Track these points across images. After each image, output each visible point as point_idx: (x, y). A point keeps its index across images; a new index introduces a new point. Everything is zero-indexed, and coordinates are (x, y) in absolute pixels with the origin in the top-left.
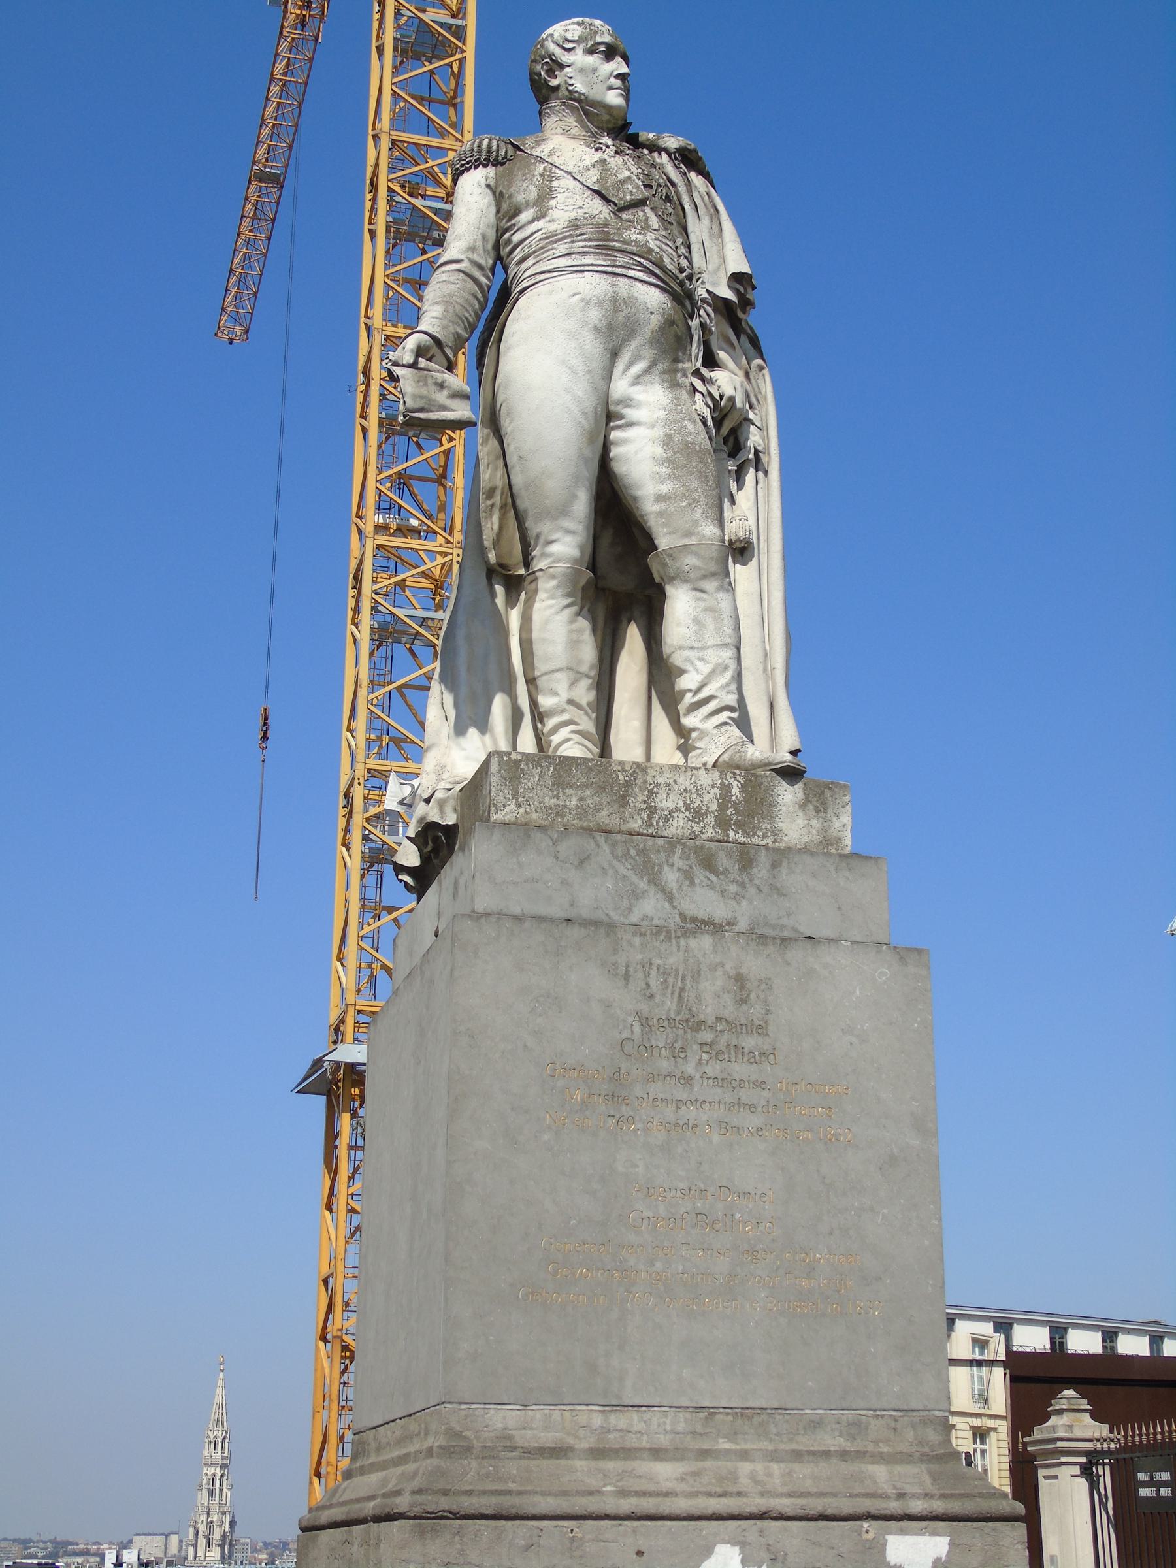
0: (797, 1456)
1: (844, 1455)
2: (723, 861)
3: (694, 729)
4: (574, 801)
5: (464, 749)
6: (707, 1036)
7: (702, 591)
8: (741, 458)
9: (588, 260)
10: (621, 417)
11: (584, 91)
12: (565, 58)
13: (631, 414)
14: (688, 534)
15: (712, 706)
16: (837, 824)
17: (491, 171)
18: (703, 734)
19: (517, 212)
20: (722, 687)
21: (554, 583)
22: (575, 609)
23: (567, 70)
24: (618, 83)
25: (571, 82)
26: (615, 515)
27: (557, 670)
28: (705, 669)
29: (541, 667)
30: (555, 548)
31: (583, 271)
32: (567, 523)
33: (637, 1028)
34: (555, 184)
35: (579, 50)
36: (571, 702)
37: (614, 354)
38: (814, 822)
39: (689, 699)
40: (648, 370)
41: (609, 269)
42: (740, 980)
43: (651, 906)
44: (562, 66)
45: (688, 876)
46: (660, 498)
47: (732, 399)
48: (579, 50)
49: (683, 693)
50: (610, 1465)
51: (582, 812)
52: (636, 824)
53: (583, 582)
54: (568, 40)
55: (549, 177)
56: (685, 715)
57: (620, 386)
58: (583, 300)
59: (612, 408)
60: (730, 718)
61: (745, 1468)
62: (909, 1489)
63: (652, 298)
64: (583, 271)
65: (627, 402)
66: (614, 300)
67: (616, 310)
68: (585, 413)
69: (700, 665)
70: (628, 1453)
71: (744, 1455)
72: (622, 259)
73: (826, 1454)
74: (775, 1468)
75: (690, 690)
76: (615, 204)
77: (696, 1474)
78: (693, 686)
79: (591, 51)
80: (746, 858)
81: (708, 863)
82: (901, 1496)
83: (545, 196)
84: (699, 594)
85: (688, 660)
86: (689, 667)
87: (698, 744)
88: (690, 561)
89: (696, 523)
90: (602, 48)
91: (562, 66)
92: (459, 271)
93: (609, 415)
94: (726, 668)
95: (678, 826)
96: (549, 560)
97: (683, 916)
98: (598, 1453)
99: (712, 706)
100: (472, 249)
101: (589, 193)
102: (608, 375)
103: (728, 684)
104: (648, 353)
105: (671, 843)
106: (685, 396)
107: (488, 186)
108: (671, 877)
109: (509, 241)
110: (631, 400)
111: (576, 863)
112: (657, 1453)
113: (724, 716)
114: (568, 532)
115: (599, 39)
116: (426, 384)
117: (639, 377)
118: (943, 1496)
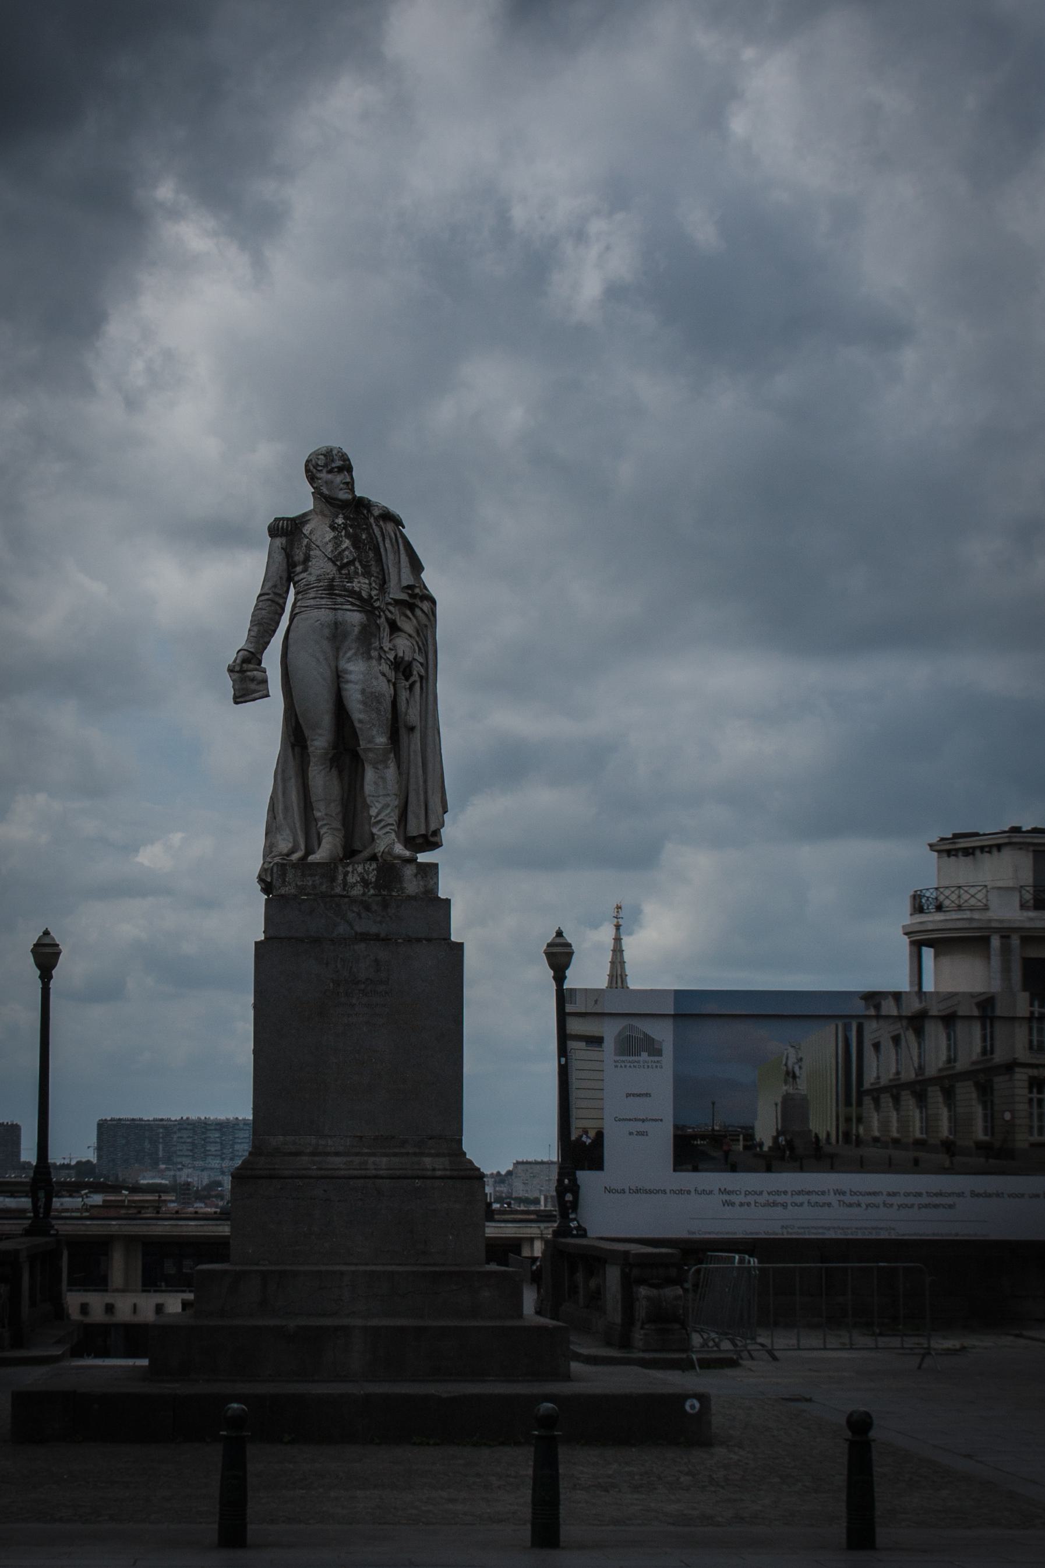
0: (395, 1155)
1: (415, 1154)
2: (374, 907)
4: (310, 883)
6: (362, 986)
8: (412, 679)
9: (323, 602)
12: (318, 475)
14: (370, 742)
15: (382, 824)
17: (283, 540)
19: (295, 566)
24: (344, 486)
28: (379, 806)
29: (313, 799)
30: (316, 743)
33: (331, 985)
34: (312, 553)
35: (324, 471)
36: (326, 815)
37: (337, 650)
38: (421, 883)
39: (373, 820)
40: (355, 654)
42: (376, 960)
43: (342, 929)
45: (359, 915)
46: (360, 721)
48: (324, 471)
50: (316, 1159)
51: (314, 887)
52: (338, 890)
53: (330, 756)
55: (308, 547)
57: (343, 664)
61: (372, 1159)
62: (437, 1167)
63: (355, 618)
65: (346, 672)
66: (336, 623)
67: (336, 628)
70: (328, 1154)
71: (373, 1155)
72: (340, 600)
73: (408, 1154)
74: (384, 1159)
77: (877, 1046)
79: (330, 472)
80: (385, 905)
81: (368, 908)
82: (434, 1170)
83: (307, 559)
88: (371, 755)
89: (373, 737)
92: (268, 600)
93: (339, 677)
95: (357, 891)
97: (356, 933)
98: (313, 1154)
99: (382, 824)
100: (275, 586)
102: (337, 658)
104: (354, 645)
105: (353, 900)
106: (374, 662)
108: (351, 916)
112: (337, 1154)
113: (387, 829)
114: (320, 735)
115: (334, 465)
118: (451, 1170)
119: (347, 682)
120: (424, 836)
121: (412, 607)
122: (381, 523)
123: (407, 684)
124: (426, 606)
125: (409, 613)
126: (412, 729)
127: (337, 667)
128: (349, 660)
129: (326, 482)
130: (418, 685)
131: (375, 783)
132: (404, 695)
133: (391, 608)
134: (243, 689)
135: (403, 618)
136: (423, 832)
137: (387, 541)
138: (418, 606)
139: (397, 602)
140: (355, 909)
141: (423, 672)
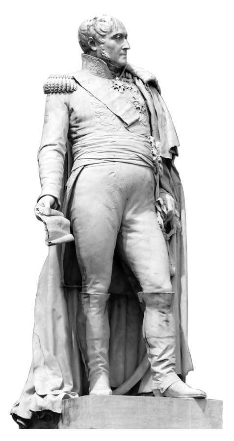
3: (158, 373)
5: (52, 370)
7: (163, 313)
10: (129, 227)
11: (109, 57)
12: (102, 40)
13: (134, 227)
18: (162, 375)
20: (170, 355)
21: (96, 301)
23: (102, 45)
25: (104, 52)
26: (123, 268)
28: (164, 347)
44: (100, 43)
47: (171, 212)
49: (152, 356)
54: (102, 31)
56: (153, 366)
57: (129, 215)
58: (115, 176)
59: (124, 223)
60: (173, 369)
65: (132, 222)
68: (113, 227)
69: (160, 344)
75: (157, 356)
76: (127, 125)
78: (158, 354)
79: (114, 37)
84: (161, 314)
85: (155, 342)
86: (156, 345)
87: (159, 379)
91: (100, 43)
94: (172, 347)
96: (94, 290)
100: (60, 138)
101: (115, 116)
103: (173, 354)
107: (66, 103)
109: (75, 133)
110: (133, 220)
113: (170, 368)
114: (104, 279)
119: (132, 231)
127: (123, 217)
128: (135, 212)
129: (109, 47)
130: (175, 238)
131: (160, 325)
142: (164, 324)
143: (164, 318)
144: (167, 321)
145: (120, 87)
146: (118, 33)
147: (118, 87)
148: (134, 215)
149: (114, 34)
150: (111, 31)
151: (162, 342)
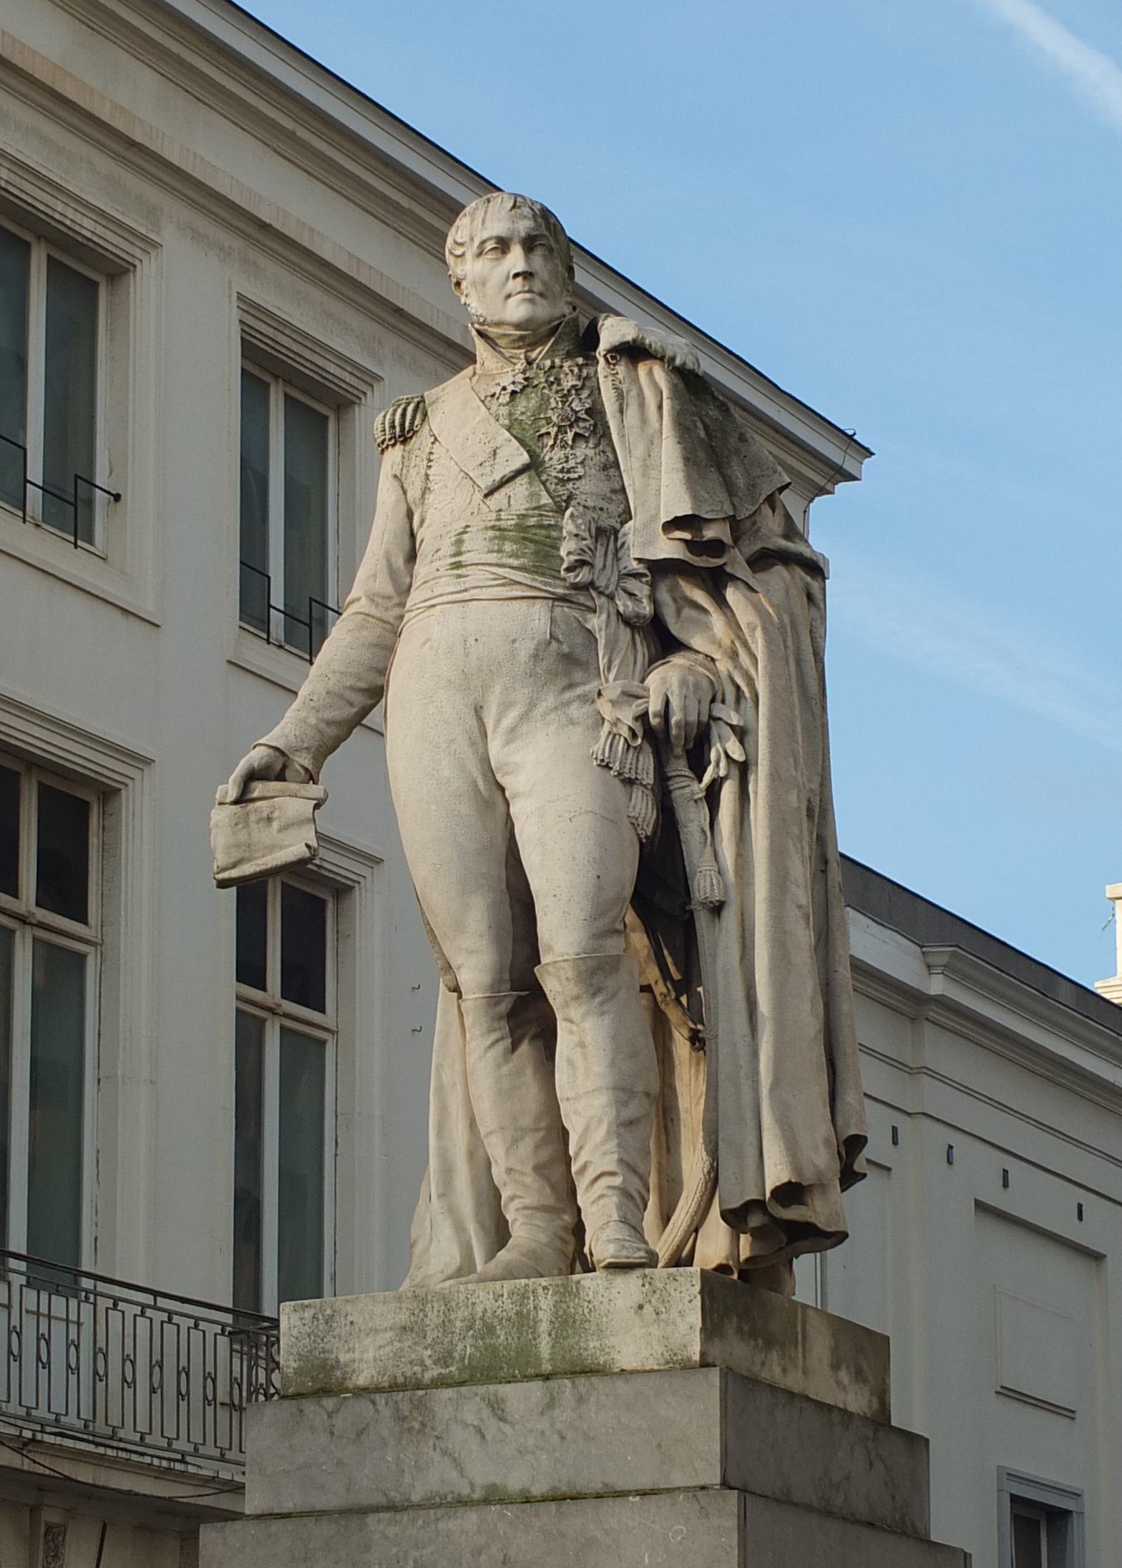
8: (707, 778)
16: (682, 1327)
22: (500, 1047)
27: (491, 1133)
31: (434, 606)
32: (468, 942)
35: (469, 256)
38: (654, 1329)
41: (459, 597)
53: (504, 1007)
58: (431, 647)
64: (434, 606)
84: (569, 1024)
90: (490, 245)
94: (600, 1122)
99: (590, 1174)
100: (375, 576)
103: (603, 1143)
107: (395, 476)
111: (353, 1437)
114: (470, 952)
116: (247, 825)
117: (513, 730)
120: (756, 1205)
121: (716, 582)
122: (621, 369)
123: (699, 789)
124: (779, 576)
125: (700, 596)
126: (717, 909)
130: (728, 794)
132: (692, 818)
133: (632, 584)
134: (237, 846)
135: (688, 612)
136: (753, 1195)
137: (632, 412)
138: (733, 578)
139: (659, 569)
140: (470, 1418)
141: (738, 755)
142: (577, 1056)
143: (575, 1039)
144: (582, 1045)
145: (504, 388)
146: (485, 235)
147: (498, 390)
148: (512, 746)
149: (476, 243)
150: (472, 239)
151: (576, 1113)
